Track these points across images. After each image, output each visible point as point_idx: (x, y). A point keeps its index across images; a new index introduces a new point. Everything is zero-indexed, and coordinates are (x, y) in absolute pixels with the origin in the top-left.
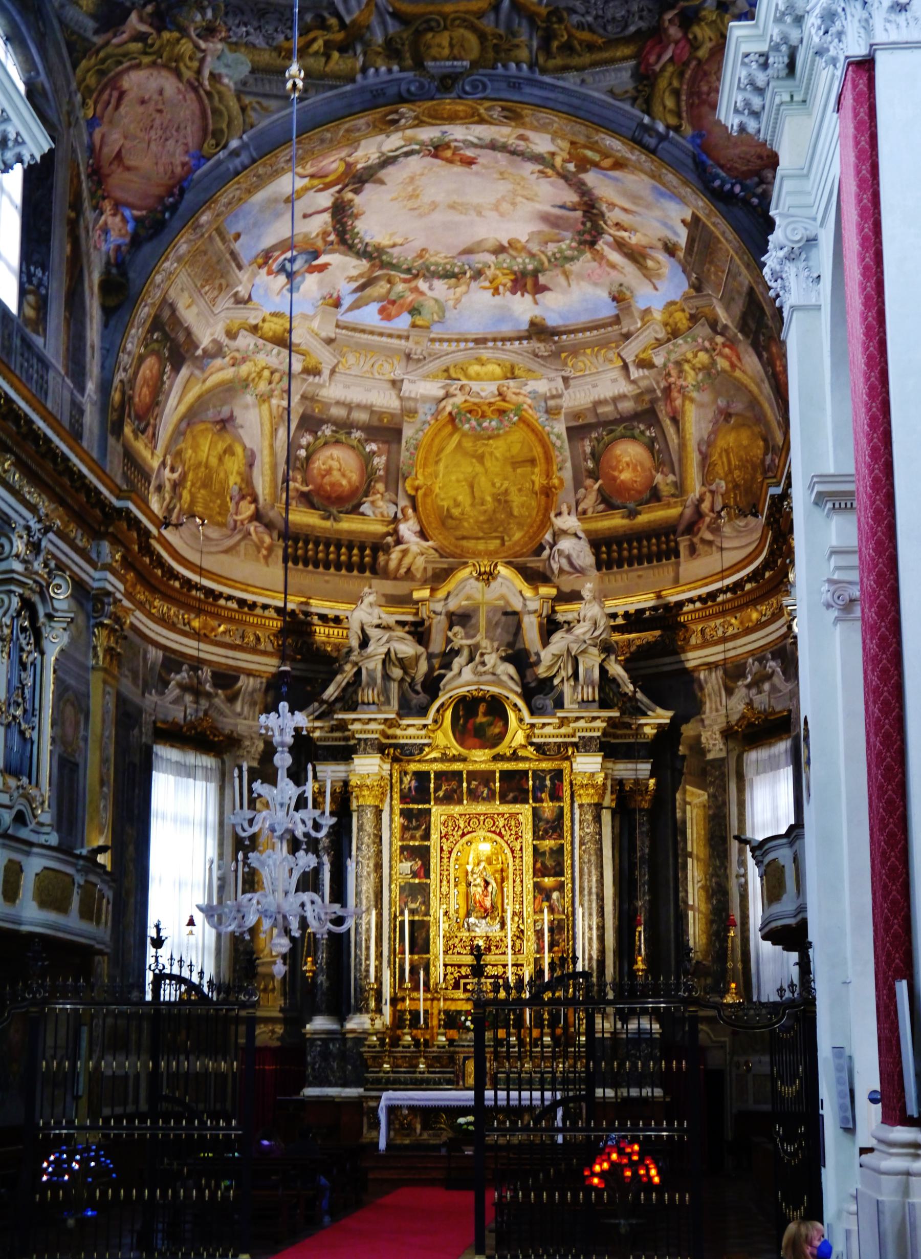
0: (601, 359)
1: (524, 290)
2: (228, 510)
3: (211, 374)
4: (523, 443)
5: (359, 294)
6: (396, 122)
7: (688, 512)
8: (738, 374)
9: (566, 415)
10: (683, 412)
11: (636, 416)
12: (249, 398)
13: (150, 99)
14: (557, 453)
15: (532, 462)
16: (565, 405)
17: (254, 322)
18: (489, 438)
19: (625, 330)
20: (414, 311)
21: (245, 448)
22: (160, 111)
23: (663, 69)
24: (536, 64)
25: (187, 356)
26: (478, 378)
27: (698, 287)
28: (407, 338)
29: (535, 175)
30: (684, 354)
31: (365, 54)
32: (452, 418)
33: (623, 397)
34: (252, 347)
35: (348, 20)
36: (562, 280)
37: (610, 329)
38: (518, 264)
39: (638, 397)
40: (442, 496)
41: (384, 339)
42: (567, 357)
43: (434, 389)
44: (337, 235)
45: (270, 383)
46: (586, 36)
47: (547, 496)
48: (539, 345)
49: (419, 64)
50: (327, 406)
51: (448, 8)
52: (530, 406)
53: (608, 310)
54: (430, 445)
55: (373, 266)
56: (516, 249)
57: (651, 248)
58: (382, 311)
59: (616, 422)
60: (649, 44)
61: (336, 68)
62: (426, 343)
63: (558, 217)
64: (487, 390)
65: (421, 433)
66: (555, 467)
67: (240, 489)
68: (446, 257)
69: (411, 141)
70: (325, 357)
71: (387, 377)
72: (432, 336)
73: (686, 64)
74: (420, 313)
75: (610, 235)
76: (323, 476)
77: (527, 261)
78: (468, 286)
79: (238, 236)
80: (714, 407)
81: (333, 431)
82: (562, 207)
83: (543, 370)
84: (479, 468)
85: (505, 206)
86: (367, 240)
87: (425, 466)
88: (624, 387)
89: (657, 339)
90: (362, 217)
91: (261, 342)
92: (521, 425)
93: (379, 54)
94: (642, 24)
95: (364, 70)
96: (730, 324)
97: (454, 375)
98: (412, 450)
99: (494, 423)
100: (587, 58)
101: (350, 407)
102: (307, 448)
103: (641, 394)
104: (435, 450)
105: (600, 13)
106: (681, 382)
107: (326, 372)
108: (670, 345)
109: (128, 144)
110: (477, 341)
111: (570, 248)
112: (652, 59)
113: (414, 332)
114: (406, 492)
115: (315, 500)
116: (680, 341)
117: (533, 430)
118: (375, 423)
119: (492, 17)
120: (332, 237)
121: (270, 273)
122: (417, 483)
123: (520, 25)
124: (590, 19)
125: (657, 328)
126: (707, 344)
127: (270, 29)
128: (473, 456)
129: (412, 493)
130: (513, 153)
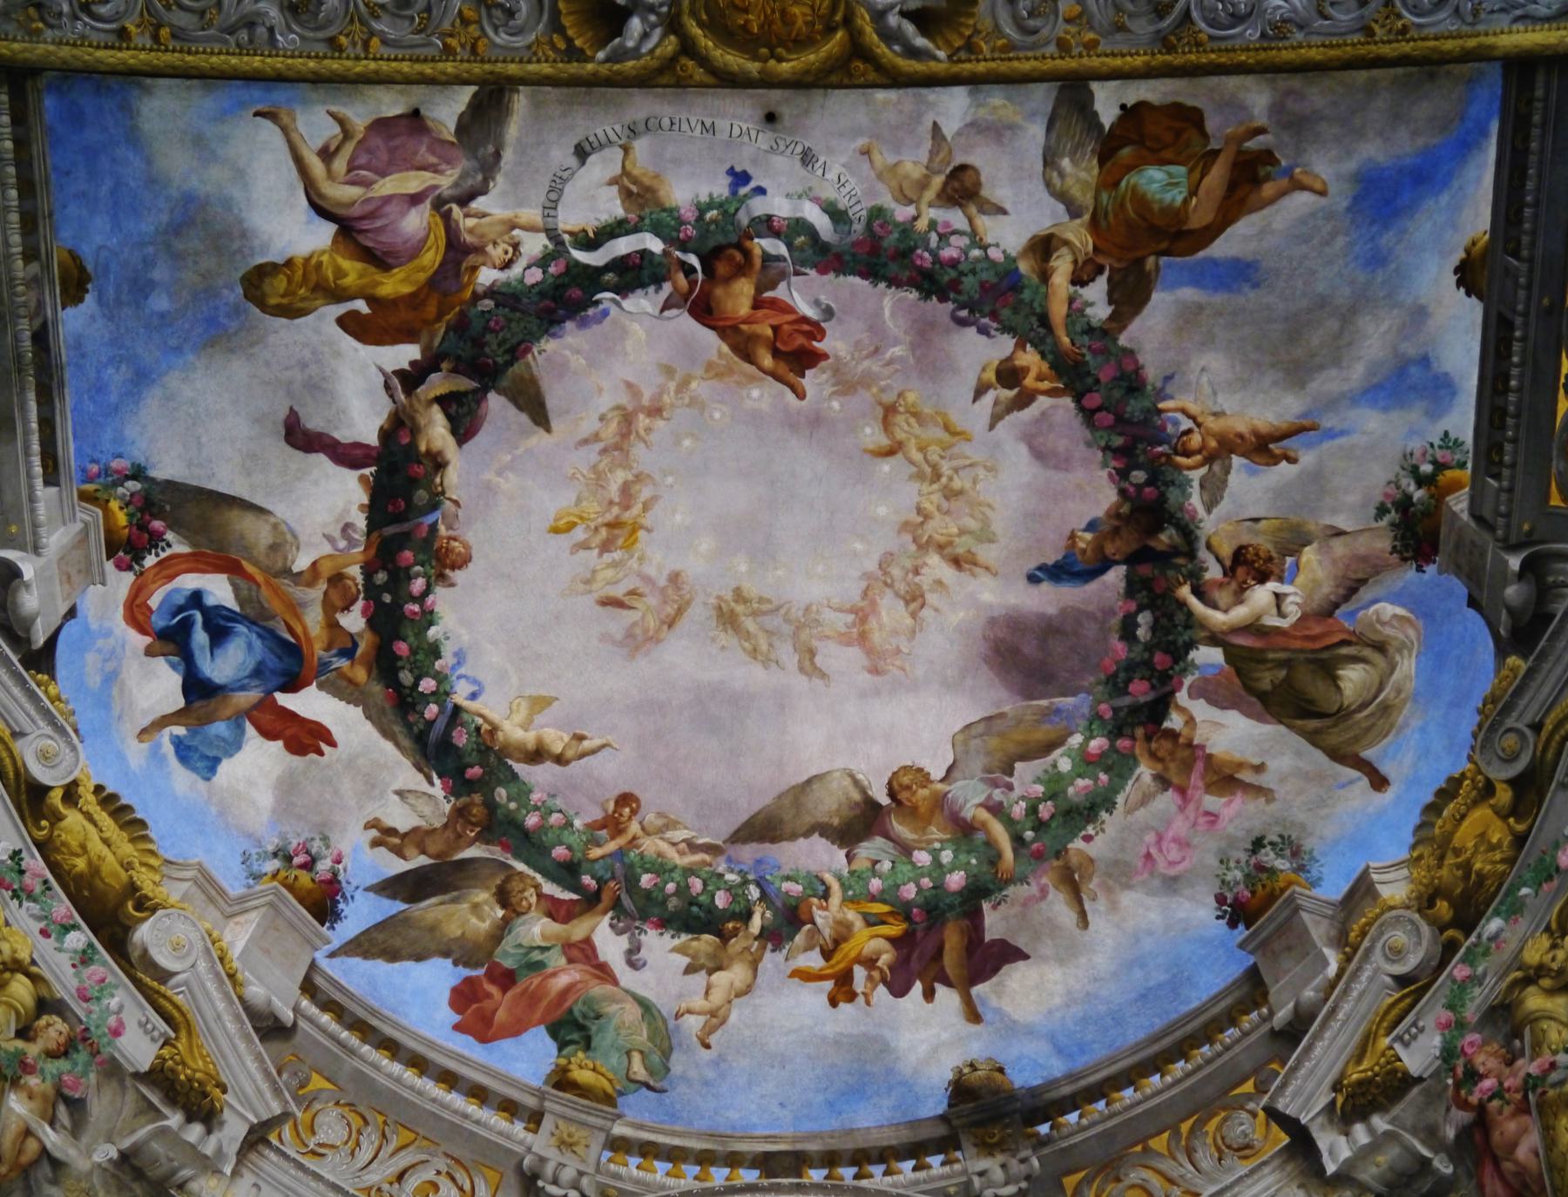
0: (1206, 1158)
1: (933, 977)
5: (399, 906)
19: (1283, 1015)
28: (535, 1119)
29: (989, 398)
30: (1517, 962)
36: (1059, 907)
37: (1233, 1032)
38: (919, 873)
41: (456, 1100)
42: (1089, 1181)
44: (372, 623)
45: (24, 1033)
48: (992, 1164)
55: (460, 813)
58: (463, 997)
62: (594, 1147)
63: (1049, 629)
68: (693, 847)
72: (619, 1130)
74: (587, 1045)
75: (1214, 640)
77: (947, 856)
78: (754, 965)
79: (75, 285)
82: (1059, 572)
85: (891, 611)
89: (1402, 981)
90: (458, 576)
91: (35, 863)
107: (233, 1130)
108: (1458, 969)
110: (768, 1163)
111: (1087, 762)
120: (354, 621)
121: (136, 613)
125: (1399, 937)
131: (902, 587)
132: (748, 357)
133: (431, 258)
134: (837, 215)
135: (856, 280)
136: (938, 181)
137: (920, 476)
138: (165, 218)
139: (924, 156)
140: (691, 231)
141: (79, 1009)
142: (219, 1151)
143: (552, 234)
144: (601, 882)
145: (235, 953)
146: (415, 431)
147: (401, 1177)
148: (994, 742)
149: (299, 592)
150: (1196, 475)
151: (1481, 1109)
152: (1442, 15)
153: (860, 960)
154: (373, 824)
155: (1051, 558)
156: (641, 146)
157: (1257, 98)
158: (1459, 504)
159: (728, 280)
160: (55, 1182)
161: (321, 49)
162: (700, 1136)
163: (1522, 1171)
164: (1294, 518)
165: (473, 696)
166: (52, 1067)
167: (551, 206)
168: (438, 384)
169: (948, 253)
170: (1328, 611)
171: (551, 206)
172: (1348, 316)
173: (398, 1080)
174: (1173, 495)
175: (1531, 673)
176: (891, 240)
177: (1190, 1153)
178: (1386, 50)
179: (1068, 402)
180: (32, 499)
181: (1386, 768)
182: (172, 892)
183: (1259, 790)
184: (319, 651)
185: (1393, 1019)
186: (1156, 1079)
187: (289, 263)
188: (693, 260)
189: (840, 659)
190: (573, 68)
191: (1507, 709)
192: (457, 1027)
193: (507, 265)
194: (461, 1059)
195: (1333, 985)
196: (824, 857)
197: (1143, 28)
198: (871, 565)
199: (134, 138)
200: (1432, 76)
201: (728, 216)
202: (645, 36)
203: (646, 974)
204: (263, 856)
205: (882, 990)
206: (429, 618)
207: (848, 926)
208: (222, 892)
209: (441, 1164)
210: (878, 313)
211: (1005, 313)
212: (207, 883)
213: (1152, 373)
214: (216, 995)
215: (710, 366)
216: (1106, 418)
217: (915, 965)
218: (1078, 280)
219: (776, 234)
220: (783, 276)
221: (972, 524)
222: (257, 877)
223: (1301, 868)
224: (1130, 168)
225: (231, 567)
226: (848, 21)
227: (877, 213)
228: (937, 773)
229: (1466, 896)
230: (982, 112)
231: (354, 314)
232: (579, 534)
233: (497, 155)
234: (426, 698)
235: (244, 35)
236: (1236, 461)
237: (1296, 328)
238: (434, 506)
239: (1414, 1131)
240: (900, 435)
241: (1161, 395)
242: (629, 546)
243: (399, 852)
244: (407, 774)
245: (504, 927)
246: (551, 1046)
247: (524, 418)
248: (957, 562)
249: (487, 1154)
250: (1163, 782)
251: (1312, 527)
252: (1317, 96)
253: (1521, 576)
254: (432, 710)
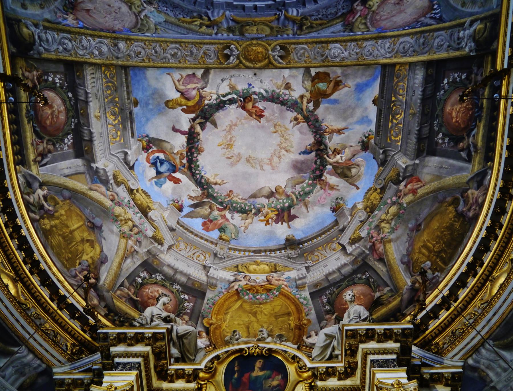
0: (328, 251)
1: (283, 221)
2: (75, 266)
3: (96, 190)
4: (282, 305)
5: (193, 209)
6: (227, 57)
7: (406, 296)
8: (420, 192)
9: (308, 286)
10: (385, 251)
11: (354, 272)
12: (115, 228)
13: (113, 7)
14: (305, 307)
15: (289, 314)
16: (308, 282)
17: (132, 187)
18: (261, 304)
19: (341, 227)
20: (222, 229)
21: (102, 251)
22: (116, 13)
23: (357, 19)
24: (296, 33)
25: (86, 156)
26: (255, 272)
27: (383, 163)
28: (216, 244)
29: (292, 123)
31: (218, 30)
32: (237, 292)
33: (345, 265)
34: (126, 200)
35: (212, 19)
36: (304, 209)
37: (332, 230)
39: (353, 262)
40: (228, 330)
41: (203, 241)
42: (308, 254)
43: (229, 276)
44: (187, 161)
46: (319, 22)
47: (300, 329)
48: (292, 252)
49: (242, 34)
50: (162, 264)
51: (257, 19)
52: (286, 286)
53: (329, 218)
54: (223, 304)
55: (203, 193)
56: (279, 193)
57: (354, 156)
58: (204, 224)
59: (342, 281)
60: (348, 16)
61: (204, 31)
63: (302, 162)
64: (260, 279)
65: (217, 297)
66: (304, 315)
67: (89, 266)
68: (242, 199)
69: (233, 88)
70: (168, 239)
71: (201, 263)
72: (230, 246)
73: (368, 14)
74: (225, 232)
75: (330, 164)
76: (149, 299)
77: (285, 201)
78: (253, 219)
79: (136, 104)
80: (408, 231)
81: (162, 279)
82: (304, 153)
83: (294, 265)
84: (253, 319)
85: (276, 159)
86: (203, 174)
87: (218, 314)
88: (344, 260)
89: (361, 221)
90: (202, 153)
91: (132, 202)
92: (281, 296)
93: (224, 30)
94: (344, 11)
95: (216, 34)
96: (410, 162)
97: (241, 270)
98: (210, 305)
99: (263, 296)
100: (320, 28)
101: (176, 271)
102: (144, 279)
103: (356, 258)
104: (225, 307)
105: (325, 13)
106: (382, 236)
107: (166, 246)
109: (94, 11)
110: (255, 252)
111: (309, 185)
112: (351, 19)
113: (220, 242)
114: (203, 324)
115: (139, 306)
116: (376, 212)
117: (288, 298)
118: (190, 284)
119: (276, 22)
120: (185, 161)
121: (148, 160)
122: (211, 321)
123: (288, 23)
124: (320, 16)
125: (361, 214)
126: (394, 199)
127: (177, 13)
128: (250, 313)
129: (208, 326)
130: (283, 103)
131: (277, 155)
132: (251, 116)
133: (197, 99)
134: (266, 91)
135: (270, 103)
136: (284, 85)
137: (280, 136)
138: (151, 92)
139: (282, 81)
140: (241, 94)
141: (140, 226)
142: (164, 250)
143: (218, 95)
144: (227, 205)
145: (166, 217)
146: (194, 129)
147: (194, 254)
148: (293, 182)
149: (175, 156)
150: (327, 136)
151: (374, 243)
152: (371, 57)
153: (270, 218)
154: (188, 195)
155: (303, 150)
156: (233, 79)
157: (339, 71)
158: (372, 141)
159: (248, 102)
160: (137, 255)
161: (178, 62)
162: (243, 247)
163: (380, 253)
164: (344, 144)
165: (205, 174)
166: (136, 236)
167: (217, 90)
168: (198, 121)
169: (285, 98)
170: (350, 159)
171: (217, 90)
172: (354, 109)
173: (193, 238)
174: (324, 140)
175: (384, 170)
176: (276, 96)
177: (325, 250)
178: (361, 63)
179: (306, 124)
180: (130, 141)
181: (359, 186)
182: (154, 207)
183: (338, 190)
184: (179, 166)
185: (360, 228)
186: (320, 238)
187: (173, 100)
188: (242, 99)
189: (267, 167)
190: (221, 66)
191: (379, 176)
192: (203, 229)
193: (210, 100)
194: (203, 234)
195: (349, 222)
196: (264, 201)
197: (319, 59)
198: (272, 152)
199: (145, 78)
200: (369, 67)
201: (248, 92)
202: (233, 60)
203: (234, 220)
204: (170, 201)
205: (274, 223)
206: (197, 161)
207: (268, 212)
208: (163, 207)
209: (201, 252)
210: (274, 108)
211: (295, 108)
212: (160, 205)
213: (320, 119)
214: (163, 224)
215: (245, 117)
216: (312, 126)
217: (279, 218)
218: (308, 103)
219: (256, 95)
220: (257, 102)
221: (289, 145)
222: (169, 204)
223: (344, 203)
224: (317, 83)
225: (164, 152)
226: (268, 57)
227: (273, 91)
228: (283, 187)
229: (372, 208)
230: (292, 74)
231: (184, 109)
232: (223, 146)
233: (208, 81)
234: (197, 174)
235: (164, 60)
236: (334, 134)
237: (345, 111)
238: (198, 141)
239: (363, 246)
240: (277, 129)
241: (322, 122)
242: (231, 148)
243: (193, 200)
244: (193, 186)
245: (211, 212)
246: (219, 232)
247: (213, 126)
248: (287, 151)
249: (208, 250)
250: (321, 188)
251: (347, 145)
252: (349, 71)
253: (382, 154)
254: (198, 176)
